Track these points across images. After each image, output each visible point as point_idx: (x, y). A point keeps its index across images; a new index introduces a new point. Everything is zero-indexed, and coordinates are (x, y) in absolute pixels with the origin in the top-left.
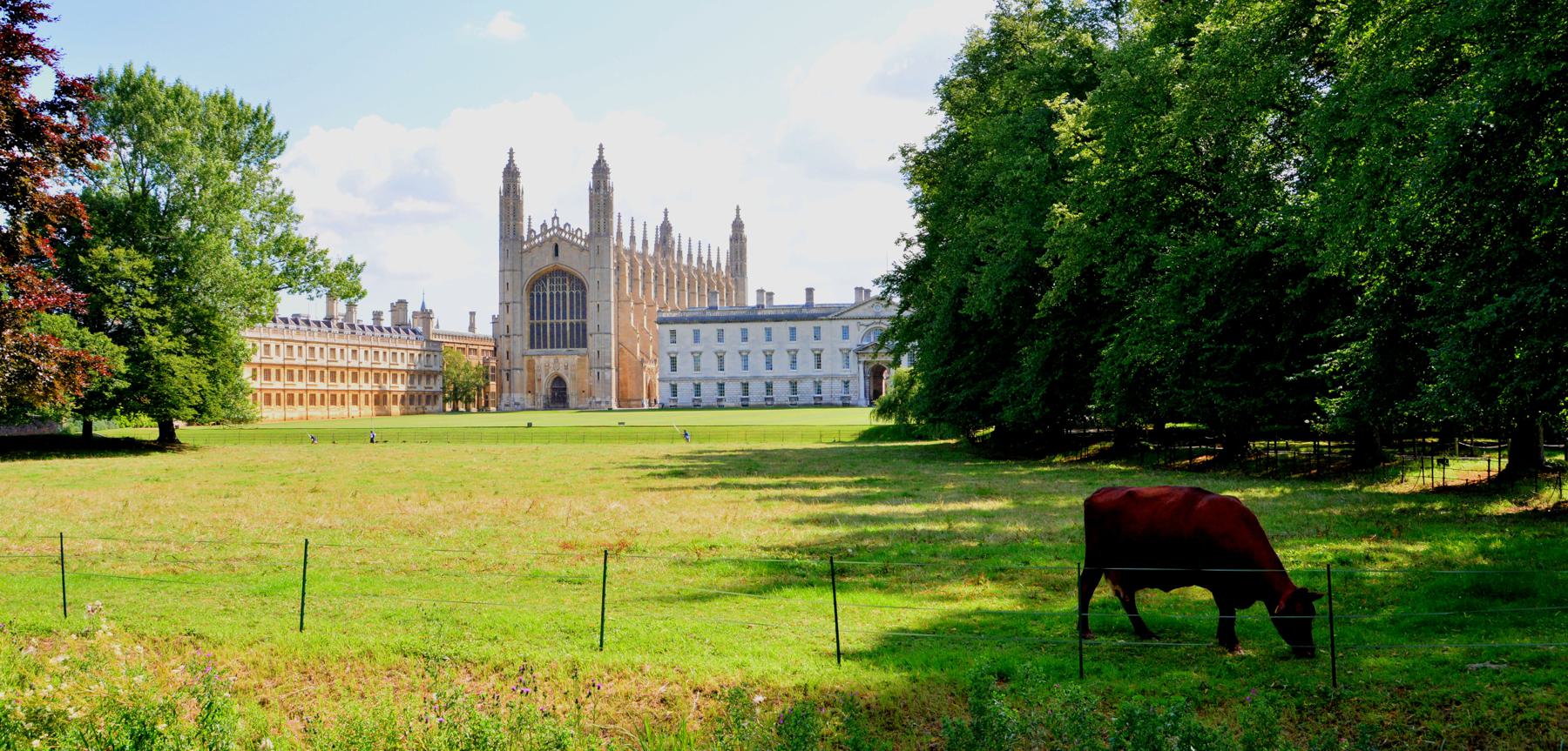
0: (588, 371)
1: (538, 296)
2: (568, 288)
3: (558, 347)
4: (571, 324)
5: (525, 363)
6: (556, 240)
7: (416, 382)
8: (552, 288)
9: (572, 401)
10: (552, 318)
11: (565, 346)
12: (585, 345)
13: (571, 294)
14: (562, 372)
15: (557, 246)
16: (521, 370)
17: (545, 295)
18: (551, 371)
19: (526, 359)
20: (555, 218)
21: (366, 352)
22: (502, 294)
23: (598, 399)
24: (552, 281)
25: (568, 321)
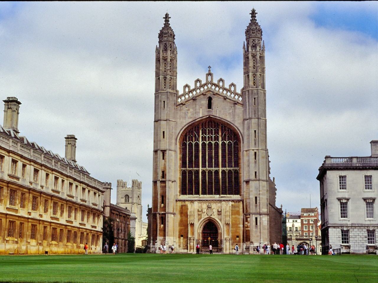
0: (242, 217)
1: (191, 145)
2: (220, 139)
3: (211, 193)
4: (223, 172)
5: (178, 208)
6: (209, 95)
7: (85, 219)
8: (204, 139)
9: (227, 247)
10: (204, 166)
11: (217, 192)
12: (237, 191)
13: (223, 144)
14: (215, 217)
15: (210, 99)
16: (174, 214)
17: (197, 145)
18: (204, 216)
19: (179, 204)
20: (210, 74)
21: (47, 175)
22: (156, 141)
23: (256, 244)
24: (204, 132)
25: (221, 169)
